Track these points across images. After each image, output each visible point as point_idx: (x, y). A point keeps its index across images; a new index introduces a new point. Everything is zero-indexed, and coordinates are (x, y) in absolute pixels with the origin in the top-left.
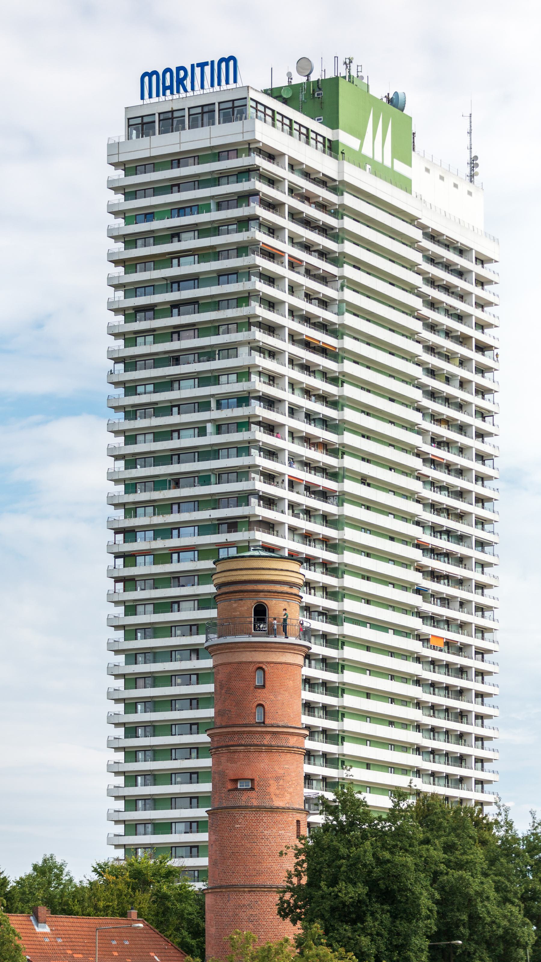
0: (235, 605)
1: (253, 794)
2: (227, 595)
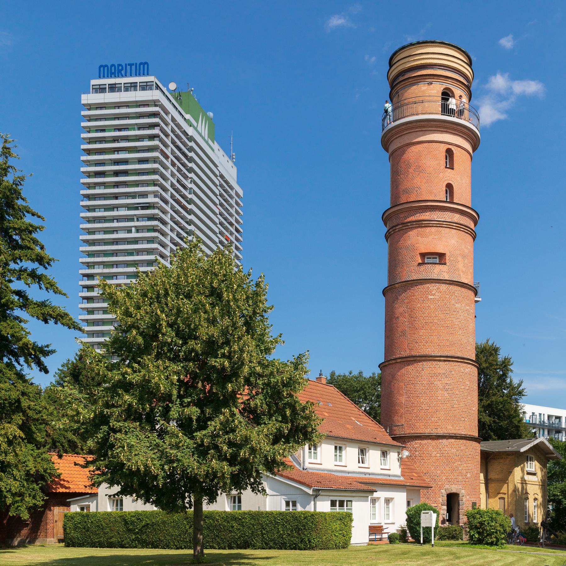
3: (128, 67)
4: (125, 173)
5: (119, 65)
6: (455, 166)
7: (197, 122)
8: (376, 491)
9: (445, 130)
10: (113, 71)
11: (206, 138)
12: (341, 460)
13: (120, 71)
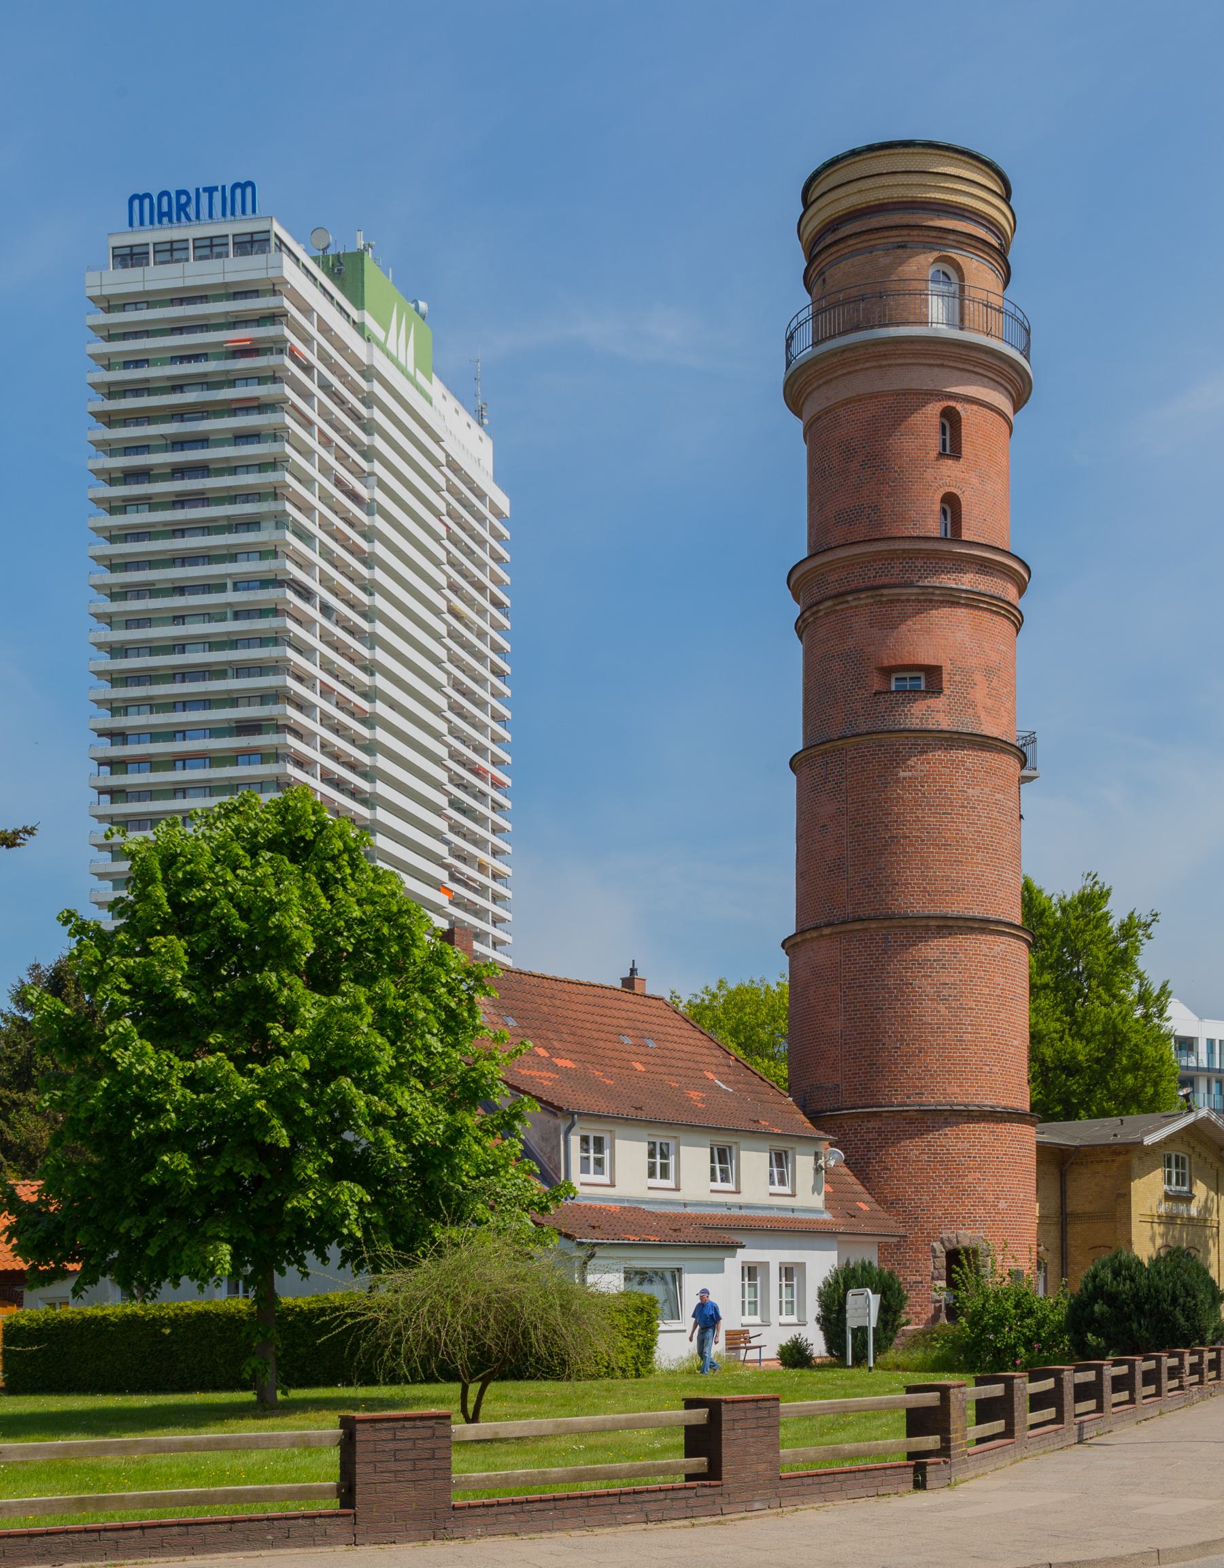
0: (885, 261)
1: (938, 703)
2: (865, 237)
3: (204, 197)
4: (202, 469)
5: (179, 193)
6: (966, 448)
7: (387, 329)
8: (743, 1247)
9: (939, 362)
10: (165, 208)
11: (411, 368)
12: (665, 1175)
13: (182, 208)
